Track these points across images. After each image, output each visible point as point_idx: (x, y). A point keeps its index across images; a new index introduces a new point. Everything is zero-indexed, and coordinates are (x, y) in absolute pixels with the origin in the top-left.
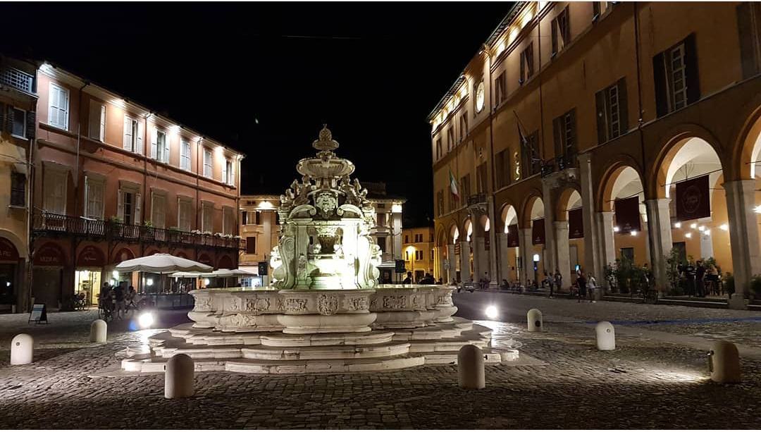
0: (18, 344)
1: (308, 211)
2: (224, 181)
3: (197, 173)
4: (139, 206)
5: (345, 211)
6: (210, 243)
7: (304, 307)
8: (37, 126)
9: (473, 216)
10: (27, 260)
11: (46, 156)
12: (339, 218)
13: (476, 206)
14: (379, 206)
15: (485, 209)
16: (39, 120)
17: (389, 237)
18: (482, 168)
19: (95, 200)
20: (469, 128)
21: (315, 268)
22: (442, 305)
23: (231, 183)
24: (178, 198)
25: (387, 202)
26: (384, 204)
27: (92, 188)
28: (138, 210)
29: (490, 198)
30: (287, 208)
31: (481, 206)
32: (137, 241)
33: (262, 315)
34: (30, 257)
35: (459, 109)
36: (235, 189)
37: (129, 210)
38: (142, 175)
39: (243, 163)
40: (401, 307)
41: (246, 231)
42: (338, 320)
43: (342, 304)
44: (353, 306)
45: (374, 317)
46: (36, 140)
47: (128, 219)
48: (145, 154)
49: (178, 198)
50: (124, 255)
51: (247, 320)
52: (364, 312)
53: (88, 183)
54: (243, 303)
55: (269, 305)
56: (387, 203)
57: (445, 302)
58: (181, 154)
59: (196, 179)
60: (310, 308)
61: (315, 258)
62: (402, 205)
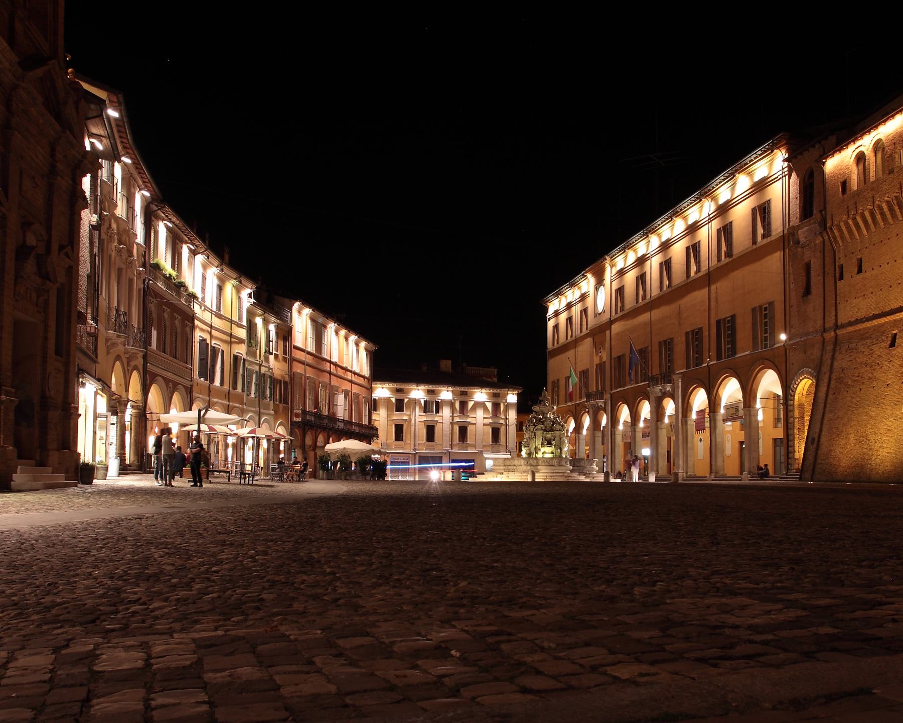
9: (591, 411)
12: (553, 431)
13: (593, 402)
14: (495, 395)
15: (603, 406)
18: (601, 367)
20: (589, 326)
29: (607, 396)
31: (601, 403)
35: (580, 301)
42: (561, 468)
56: (502, 392)
57: (593, 465)
58: (345, 353)
60: (551, 464)
62: (518, 395)
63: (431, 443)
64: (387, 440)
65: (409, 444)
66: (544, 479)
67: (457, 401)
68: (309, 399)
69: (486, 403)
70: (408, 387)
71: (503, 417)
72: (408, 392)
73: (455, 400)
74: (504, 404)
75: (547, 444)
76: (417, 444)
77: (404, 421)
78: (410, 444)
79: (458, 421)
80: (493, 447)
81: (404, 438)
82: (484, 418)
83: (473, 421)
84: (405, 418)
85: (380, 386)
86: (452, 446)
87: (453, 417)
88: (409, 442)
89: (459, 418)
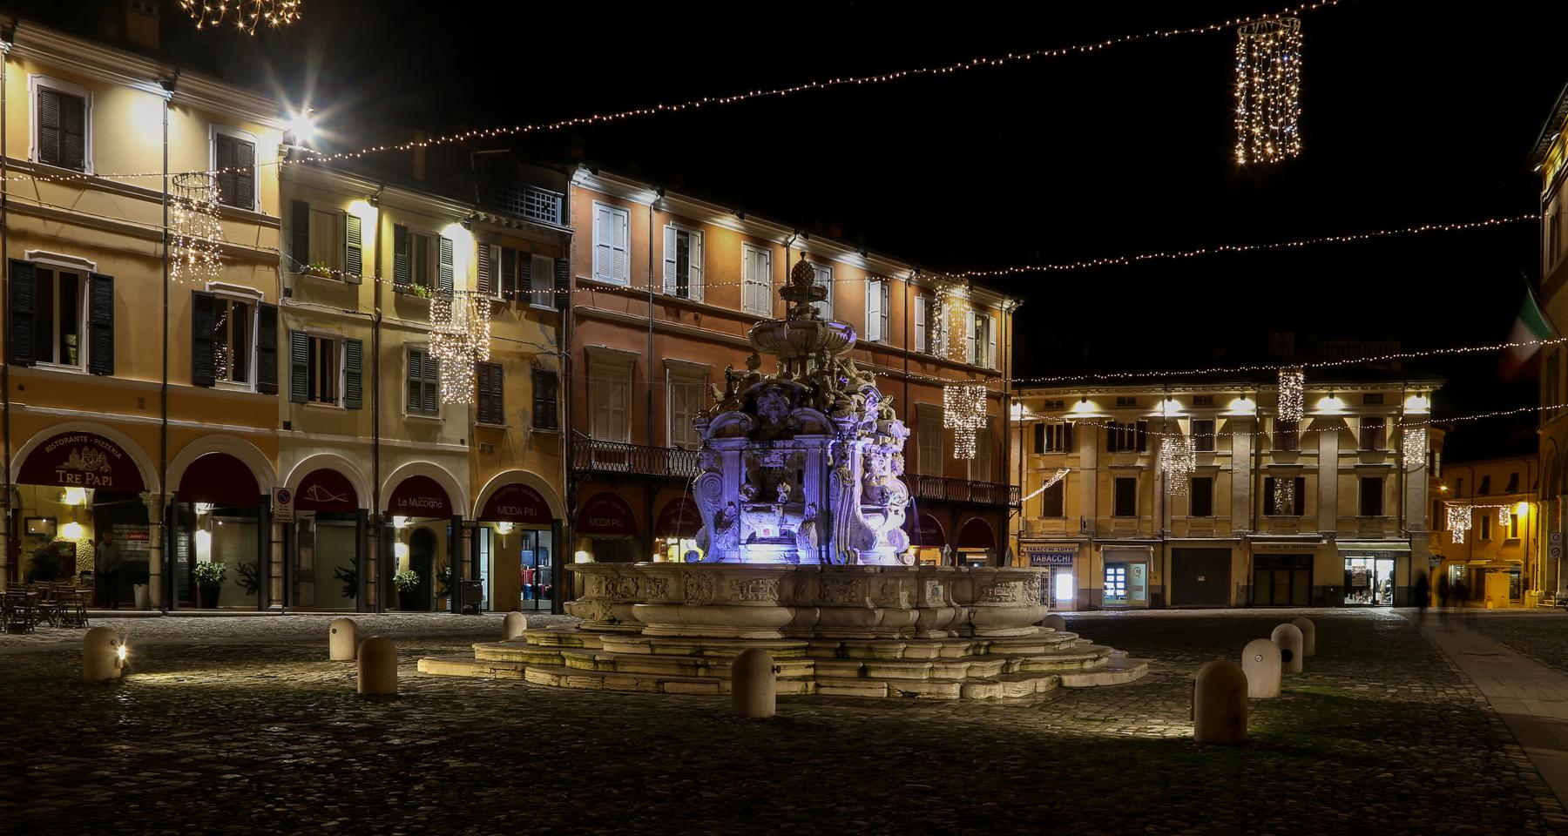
2: (970, 359)
3: (906, 347)
7: (663, 592)
8: (573, 284)
10: (565, 523)
11: (594, 338)
16: (577, 274)
17: (1393, 476)
19: (686, 412)
21: (752, 532)
23: (989, 362)
25: (1391, 389)
26: (1381, 395)
27: (680, 391)
34: (570, 520)
36: (999, 375)
39: (1018, 317)
40: (850, 601)
41: (1042, 466)
42: (706, 615)
43: (720, 589)
45: (786, 615)
46: (571, 310)
55: (638, 587)
60: (672, 593)
62: (1434, 397)
64: (1096, 516)
65: (1149, 521)
67: (1268, 419)
68: (677, 417)
70: (1145, 394)
71: (1393, 451)
72: (1149, 403)
73: (1263, 418)
74: (1395, 421)
75: (752, 501)
76: (1168, 521)
78: (1151, 522)
80: (1364, 525)
81: (1137, 509)
82: (1340, 456)
83: (1312, 463)
84: (1140, 463)
85: (1080, 395)
86: (1255, 525)
87: (1258, 457)
88: (1149, 517)
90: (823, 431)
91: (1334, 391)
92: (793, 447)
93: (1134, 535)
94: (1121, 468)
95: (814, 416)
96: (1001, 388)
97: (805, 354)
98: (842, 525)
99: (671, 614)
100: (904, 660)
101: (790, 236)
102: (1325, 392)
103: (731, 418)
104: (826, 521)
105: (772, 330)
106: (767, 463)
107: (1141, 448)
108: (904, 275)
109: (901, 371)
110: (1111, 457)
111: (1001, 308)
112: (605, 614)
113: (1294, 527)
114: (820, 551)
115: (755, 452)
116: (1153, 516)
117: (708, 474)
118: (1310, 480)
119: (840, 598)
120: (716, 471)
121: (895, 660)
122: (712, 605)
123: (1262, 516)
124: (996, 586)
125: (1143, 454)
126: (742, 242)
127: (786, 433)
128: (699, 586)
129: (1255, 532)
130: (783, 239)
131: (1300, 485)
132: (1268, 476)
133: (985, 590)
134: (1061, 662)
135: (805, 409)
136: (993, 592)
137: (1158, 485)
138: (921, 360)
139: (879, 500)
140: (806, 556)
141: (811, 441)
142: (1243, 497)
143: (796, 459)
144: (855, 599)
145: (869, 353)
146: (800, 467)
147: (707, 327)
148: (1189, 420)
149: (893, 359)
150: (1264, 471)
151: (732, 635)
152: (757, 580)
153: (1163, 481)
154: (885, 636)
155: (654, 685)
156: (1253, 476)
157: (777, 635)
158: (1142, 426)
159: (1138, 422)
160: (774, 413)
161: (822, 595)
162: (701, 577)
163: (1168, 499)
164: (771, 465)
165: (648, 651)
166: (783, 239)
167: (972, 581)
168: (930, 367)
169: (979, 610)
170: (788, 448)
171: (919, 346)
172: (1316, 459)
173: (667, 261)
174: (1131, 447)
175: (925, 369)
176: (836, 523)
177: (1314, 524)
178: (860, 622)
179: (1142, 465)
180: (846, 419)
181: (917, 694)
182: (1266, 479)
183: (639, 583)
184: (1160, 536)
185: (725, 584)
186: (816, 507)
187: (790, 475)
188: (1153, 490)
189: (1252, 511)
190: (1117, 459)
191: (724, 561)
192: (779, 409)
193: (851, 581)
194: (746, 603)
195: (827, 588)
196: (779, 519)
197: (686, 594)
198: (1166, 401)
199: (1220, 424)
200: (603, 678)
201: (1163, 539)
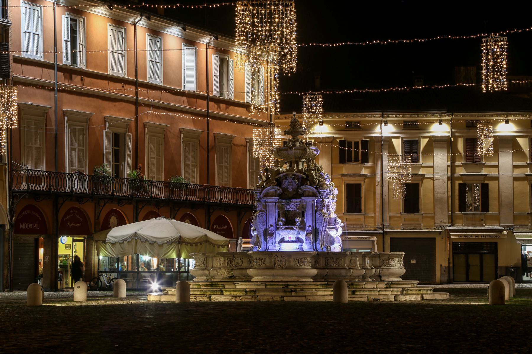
0: (79, 287)
1: (276, 191)
4: (130, 151)
5: (305, 191)
6: (228, 198)
7: (264, 263)
8: (11, 60)
10: (7, 228)
16: (13, 54)
19: (76, 147)
21: (282, 237)
22: (387, 267)
24: (181, 133)
27: (73, 132)
28: (129, 155)
30: (259, 189)
32: (129, 200)
33: (238, 269)
34: (11, 225)
37: (118, 157)
38: (133, 107)
40: (339, 266)
42: (286, 272)
43: (290, 262)
44: (297, 263)
45: (314, 271)
46: (11, 79)
47: (118, 170)
48: (136, 76)
49: (181, 133)
50: (113, 219)
51: (228, 273)
52: (307, 267)
53: (69, 126)
54: (224, 261)
55: (243, 262)
59: (205, 102)
61: (280, 229)
63: (412, 216)
65: (372, 217)
66: (236, 297)
68: (72, 150)
69: (518, 139)
73: (456, 138)
75: (284, 225)
76: (386, 217)
77: (362, 178)
78: (374, 217)
79: (462, 175)
82: (515, 167)
83: (493, 172)
84: (364, 172)
86: (452, 220)
87: (453, 167)
88: (372, 214)
89: (465, 169)
90: (314, 195)
91: (509, 118)
92: (300, 202)
93: (361, 227)
94: (351, 176)
95: (310, 189)
96: (268, 119)
97: (299, 160)
98: (323, 235)
99: (270, 272)
100: (365, 288)
101: (137, 17)
102: (502, 118)
103: (272, 189)
104: (315, 233)
105: (287, 150)
106: (289, 208)
107: (365, 160)
108: (206, 40)
109: (204, 110)
110: (343, 167)
111: (267, 60)
112: (228, 274)
113: (482, 222)
114: (313, 246)
115: (283, 203)
116: (375, 213)
117: (260, 213)
118: (492, 185)
119: (334, 265)
120: (263, 211)
121: (362, 288)
122: (287, 268)
123: (457, 212)
124: (389, 260)
125: (366, 165)
126: (108, 24)
127: (298, 195)
128: (281, 261)
129: (453, 225)
130: (132, 20)
131: (485, 189)
132: (461, 182)
133: (385, 262)
134: (420, 290)
135: (307, 186)
136: (388, 262)
137: (378, 189)
138: (217, 101)
139: (334, 223)
140: (306, 247)
141: (308, 199)
142: (442, 198)
143: (301, 207)
144: (340, 265)
145: (185, 98)
146: (303, 210)
147: (92, 86)
148: (400, 140)
149: (200, 101)
150: (458, 179)
151: (296, 280)
152: (305, 258)
153: (382, 186)
154: (353, 280)
155: (279, 298)
156: (449, 182)
157: (311, 280)
158: (365, 144)
159: (362, 141)
160: (290, 187)
161: (326, 264)
162: (282, 257)
163: (386, 199)
164: (290, 209)
165: (264, 287)
166: (132, 20)
167: (380, 258)
168: (223, 106)
169: (384, 270)
170: (298, 202)
171: (215, 92)
172: (497, 169)
173: (65, 41)
174: (357, 160)
175: (220, 108)
176: (320, 234)
177: (497, 219)
178: (344, 274)
179: (366, 174)
180: (325, 191)
181: (379, 299)
182: (460, 184)
183: (243, 260)
184: (381, 228)
185: (292, 259)
186: (311, 227)
187: (299, 213)
188: (375, 193)
189: (450, 209)
190: (347, 169)
191: (268, 251)
192: (292, 185)
193: (339, 258)
194: (300, 267)
195: (329, 261)
196: (297, 232)
197: (275, 265)
198: (383, 125)
199: (424, 142)
200: (257, 296)
201: (383, 230)
